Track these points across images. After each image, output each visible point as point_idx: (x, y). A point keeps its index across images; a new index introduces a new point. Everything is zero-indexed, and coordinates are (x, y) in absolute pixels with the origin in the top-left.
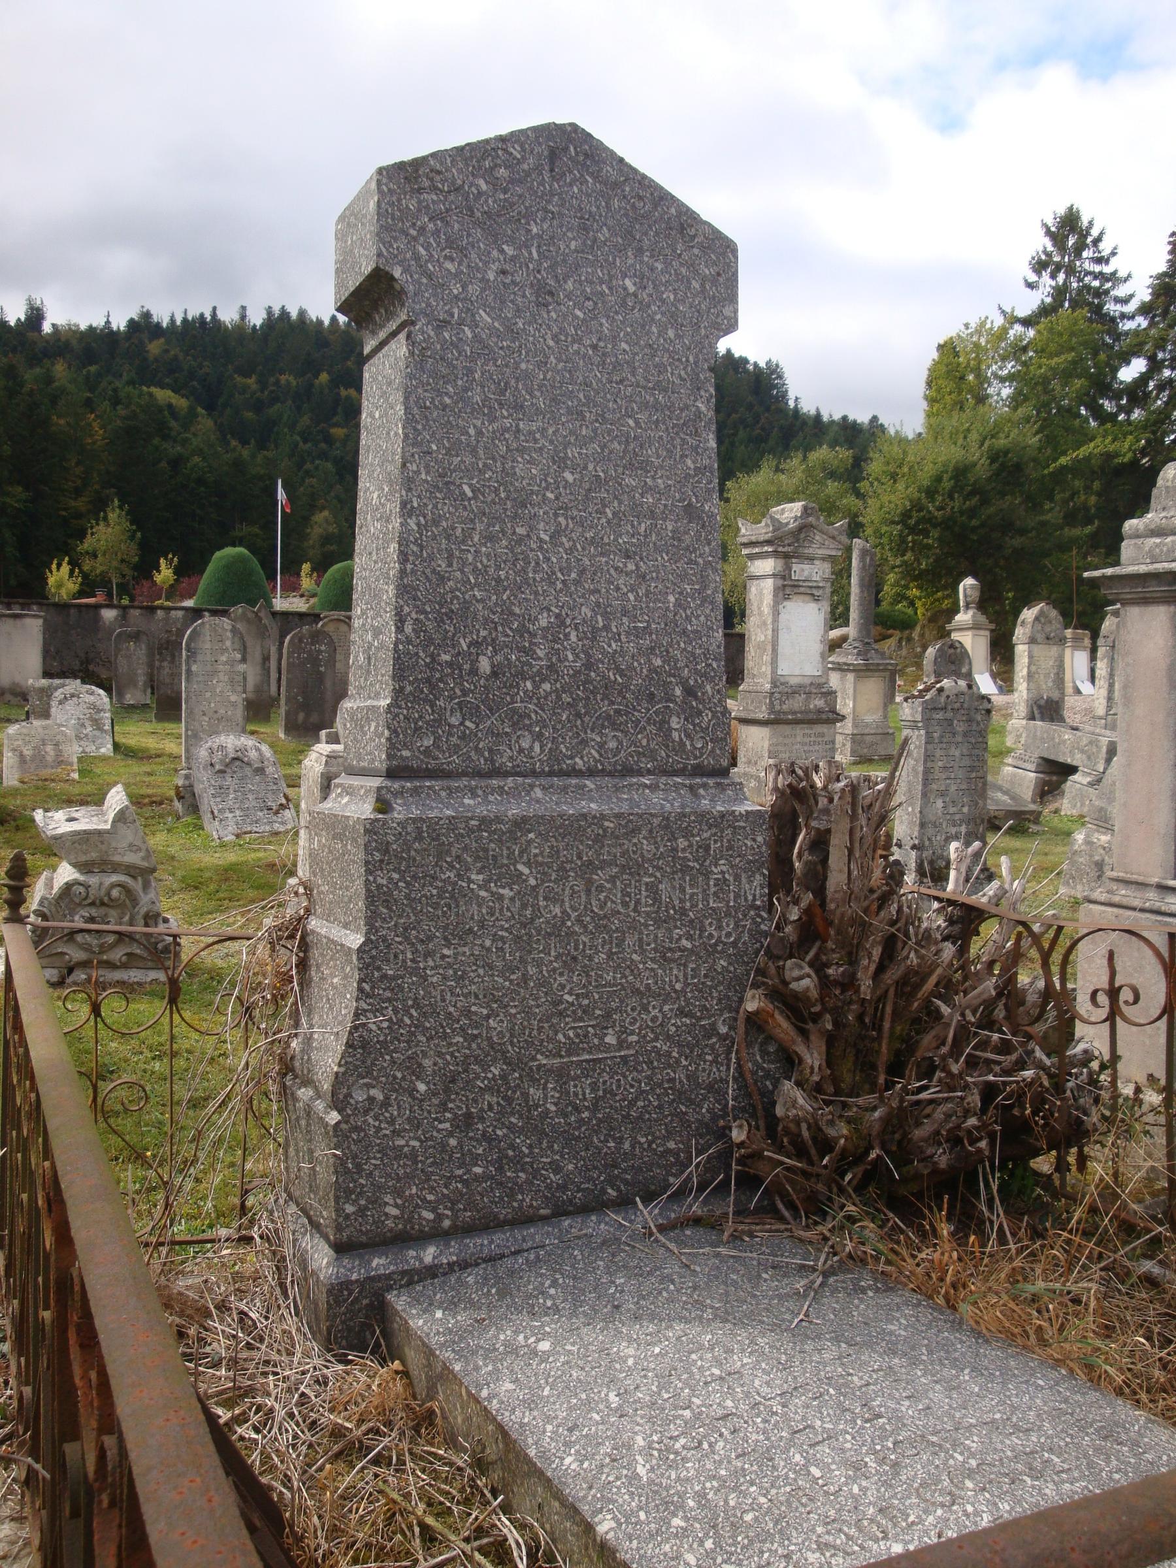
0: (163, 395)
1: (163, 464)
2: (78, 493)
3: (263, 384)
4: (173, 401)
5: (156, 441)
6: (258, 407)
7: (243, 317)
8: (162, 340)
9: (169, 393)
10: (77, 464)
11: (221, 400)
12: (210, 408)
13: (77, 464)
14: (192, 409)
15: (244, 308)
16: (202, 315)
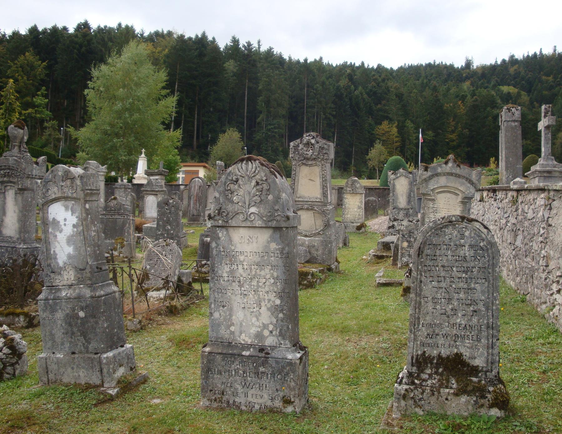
0: (505, 89)
1: (490, 118)
2: (453, 132)
3: (555, 78)
4: (511, 91)
5: (489, 109)
6: (551, 88)
7: (555, 50)
8: (517, 65)
9: (512, 87)
10: (453, 121)
11: (533, 88)
12: (529, 91)
13: (453, 121)
14: (518, 93)
15: (555, 47)
16: (535, 53)
